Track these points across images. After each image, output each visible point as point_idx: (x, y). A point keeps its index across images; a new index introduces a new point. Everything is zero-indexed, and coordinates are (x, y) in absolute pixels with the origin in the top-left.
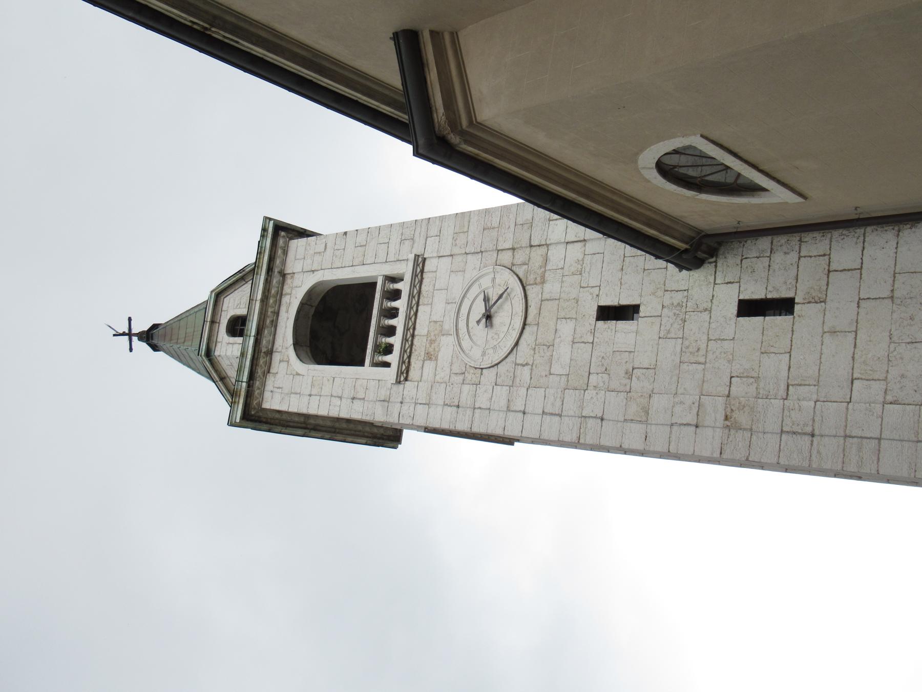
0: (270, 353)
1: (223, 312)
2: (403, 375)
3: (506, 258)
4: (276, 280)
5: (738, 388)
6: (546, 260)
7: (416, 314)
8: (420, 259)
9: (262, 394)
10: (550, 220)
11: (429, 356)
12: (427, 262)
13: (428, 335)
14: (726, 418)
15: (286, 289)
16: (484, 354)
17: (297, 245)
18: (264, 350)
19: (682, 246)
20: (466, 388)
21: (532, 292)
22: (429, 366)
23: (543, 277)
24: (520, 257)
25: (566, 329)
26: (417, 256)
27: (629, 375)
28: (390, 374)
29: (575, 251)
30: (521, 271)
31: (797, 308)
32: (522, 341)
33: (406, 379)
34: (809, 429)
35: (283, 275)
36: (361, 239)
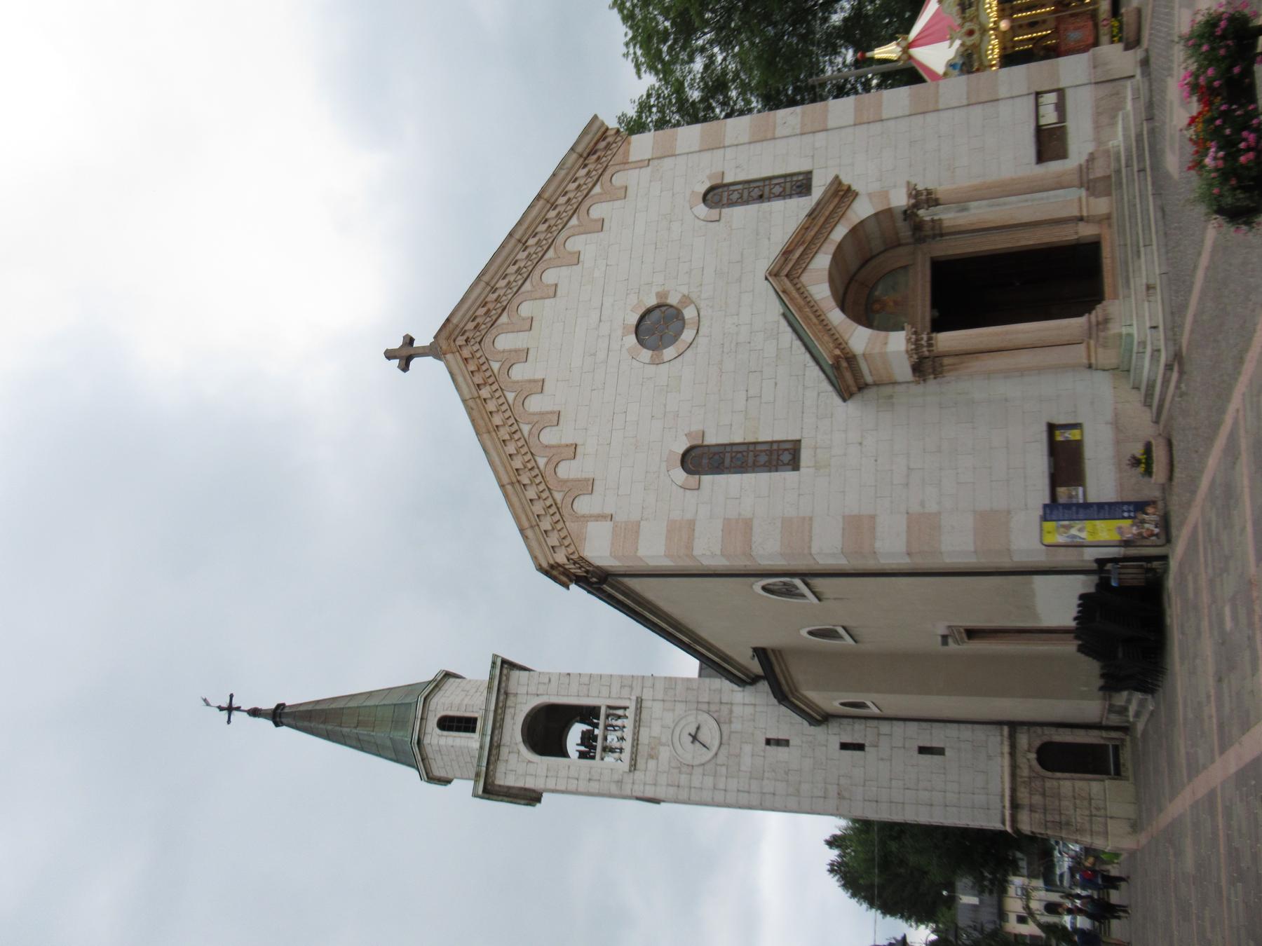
0: (499, 746)
1: (430, 713)
2: (634, 766)
3: (705, 707)
4: (502, 698)
5: (843, 781)
6: (731, 712)
7: (638, 732)
8: (639, 700)
9: (494, 775)
10: (733, 691)
11: (651, 757)
12: (643, 702)
13: (649, 744)
14: (839, 794)
15: (509, 703)
16: (694, 758)
17: (515, 674)
18: (495, 744)
19: (819, 718)
20: (683, 776)
21: (724, 727)
22: (652, 764)
23: (730, 718)
24: (713, 708)
25: (747, 749)
26: (637, 698)
27: (787, 773)
28: (625, 765)
29: (749, 710)
30: (715, 716)
31: (867, 749)
32: (720, 754)
33: (635, 769)
34: (875, 799)
35: (506, 694)
36: (586, 680)
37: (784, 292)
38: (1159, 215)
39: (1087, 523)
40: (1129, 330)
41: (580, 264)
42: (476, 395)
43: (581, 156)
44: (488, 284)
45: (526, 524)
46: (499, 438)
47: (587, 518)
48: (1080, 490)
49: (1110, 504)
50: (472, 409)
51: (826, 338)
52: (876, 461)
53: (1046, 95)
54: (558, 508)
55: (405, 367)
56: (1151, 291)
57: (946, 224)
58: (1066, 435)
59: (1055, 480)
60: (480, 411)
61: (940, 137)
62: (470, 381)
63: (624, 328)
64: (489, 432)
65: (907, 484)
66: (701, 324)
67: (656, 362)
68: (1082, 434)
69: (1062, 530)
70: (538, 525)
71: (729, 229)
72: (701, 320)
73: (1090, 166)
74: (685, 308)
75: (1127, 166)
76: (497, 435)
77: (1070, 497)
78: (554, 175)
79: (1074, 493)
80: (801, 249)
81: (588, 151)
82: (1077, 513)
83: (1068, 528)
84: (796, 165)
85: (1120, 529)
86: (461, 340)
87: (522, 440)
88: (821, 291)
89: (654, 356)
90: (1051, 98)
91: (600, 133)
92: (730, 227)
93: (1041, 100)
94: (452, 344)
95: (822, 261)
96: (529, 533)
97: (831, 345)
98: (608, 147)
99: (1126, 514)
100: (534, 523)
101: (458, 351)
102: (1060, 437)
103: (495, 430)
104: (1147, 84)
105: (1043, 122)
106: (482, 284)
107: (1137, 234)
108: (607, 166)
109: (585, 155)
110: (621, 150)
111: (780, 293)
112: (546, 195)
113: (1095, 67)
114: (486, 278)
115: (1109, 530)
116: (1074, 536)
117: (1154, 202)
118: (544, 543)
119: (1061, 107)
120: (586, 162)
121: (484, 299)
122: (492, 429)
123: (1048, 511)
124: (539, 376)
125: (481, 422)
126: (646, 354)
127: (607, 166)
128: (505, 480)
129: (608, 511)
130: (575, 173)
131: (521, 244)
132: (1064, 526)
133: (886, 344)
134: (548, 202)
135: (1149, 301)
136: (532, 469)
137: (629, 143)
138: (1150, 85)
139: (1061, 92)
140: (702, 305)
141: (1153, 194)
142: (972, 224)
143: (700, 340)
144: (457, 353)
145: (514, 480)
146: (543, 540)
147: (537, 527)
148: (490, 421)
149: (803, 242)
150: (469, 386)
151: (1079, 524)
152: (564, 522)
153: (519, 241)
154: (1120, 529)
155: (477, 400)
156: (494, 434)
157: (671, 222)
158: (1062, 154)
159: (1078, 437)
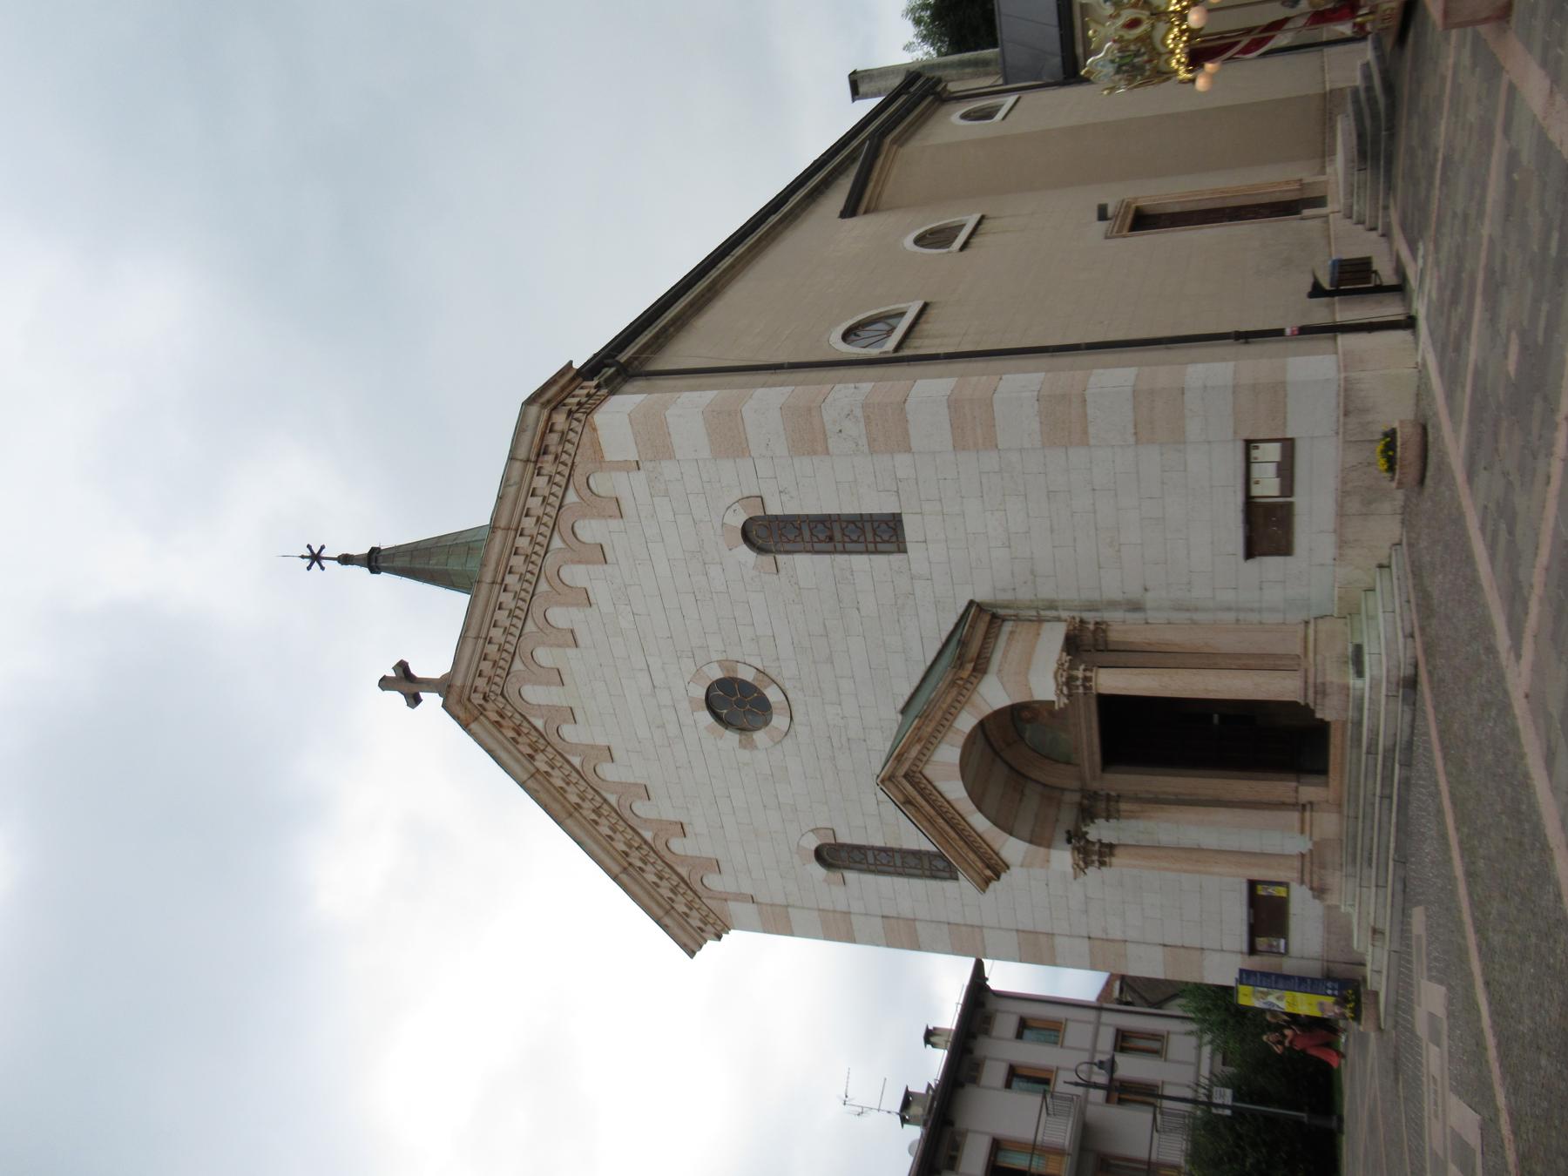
37: (904, 804)
38: (1399, 887)
39: (1287, 993)
40: (1350, 910)
41: (594, 606)
42: (533, 770)
43: (528, 461)
44: (477, 638)
45: (660, 913)
46: (585, 818)
47: (724, 898)
48: (1282, 942)
49: (1313, 980)
50: (536, 791)
51: (972, 856)
52: (1047, 885)
53: (1262, 445)
54: (687, 884)
55: (414, 700)
56: (1377, 936)
57: (1114, 636)
58: (1270, 890)
59: (1254, 931)
60: (548, 791)
61: (1094, 490)
62: (515, 752)
63: (690, 702)
64: (571, 815)
65: (1086, 911)
66: (793, 709)
67: (749, 745)
68: (1288, 892)
69: (1259, 995)
70: (673, 908)
71: (796, 586)
72: (792, 703)
73: (1318, 701)
74: (766, 688)
75: (1368, 753)
76: (581, 814)
77: (1271, 946)
78: (500, 498)
79: (1275, 943)
80: (918, 747)
81: (535, 451)
82: (1276, 982)
83: (1267, 994)
84: (874, 503)
85: (1321, 1004)
86: (477, 699)
87: (613, 814)
88: (954, 790)
89: (744, 742)
90: (1271, 452)
91: (542, 424)
92: (796, 583)
93: (1254, 453)
94: (469, 706)
95: (948, 754)
96: (667, 921)
97: (980, 864)
98: (564, 438)
99: (1329, 992)
100: (668, 907)
101: (481, 714)
102: (1261, 891)
103: (575, 809)
104: (1408, 717)
105: (1256, 491)
106: (470, 643)
107: (1372, 839)
108: (573, 463)
109: (533, 458)
110: (585, 439)
111: (901, 806)
112: (503, 523)
113: (1346, 414)
114: (472, 633)
115: (1310, 1004)
116: (1272, 1004)
117: (1394, 870)
118: (687, 926)
119: (1286, 470)
120: (539, 465)
121: (482, 651)
122: (572, 810)
123: (1244, 976)
124: (601, 741)
125: (556, 807)
126: (731, 737)
127: (573, 463)
128: (616, 869)
129: (747, 889)
130: (531, 483)
131: (498, 586)
132: (1262, 992)
133: (1048, 861)
134: (509, 529)
135: (1373, 945)
136: (638, 848)
137: (595, 429)
138: (1413, 720)
139: (1288, 445)
140: (787, 686)
141: (1394, 860)
142: (1150, 644)
143: (797, 727)
144: (482, 717)
145: (626, 865)
146: (685, 924)
147: (672, 912)
148: (565, 798)
149: (919, 740)
150: (517, 761)
151: (1277, 993)
152: (700, 898)
153: (493, 583)
154: (1321, 1004)
155: (539, 777)
156: (577, 814)
157: (705, 564)
158: (1283, 547)
159: (1284, 895)
